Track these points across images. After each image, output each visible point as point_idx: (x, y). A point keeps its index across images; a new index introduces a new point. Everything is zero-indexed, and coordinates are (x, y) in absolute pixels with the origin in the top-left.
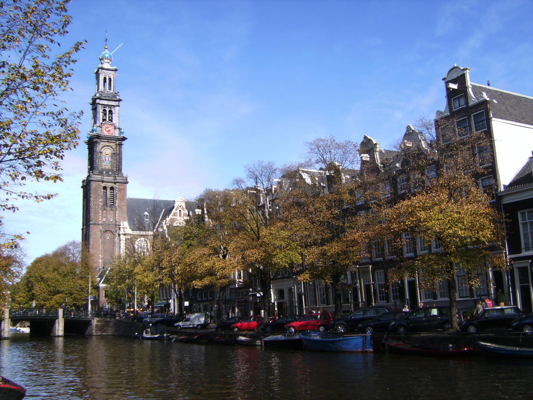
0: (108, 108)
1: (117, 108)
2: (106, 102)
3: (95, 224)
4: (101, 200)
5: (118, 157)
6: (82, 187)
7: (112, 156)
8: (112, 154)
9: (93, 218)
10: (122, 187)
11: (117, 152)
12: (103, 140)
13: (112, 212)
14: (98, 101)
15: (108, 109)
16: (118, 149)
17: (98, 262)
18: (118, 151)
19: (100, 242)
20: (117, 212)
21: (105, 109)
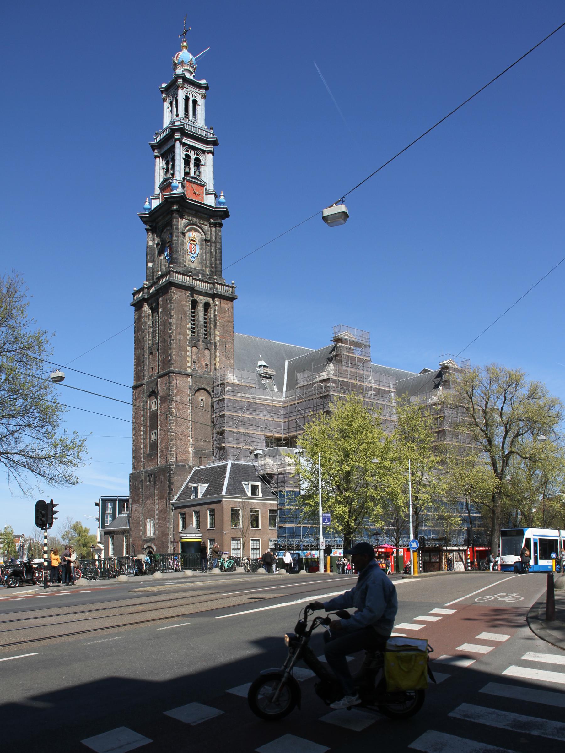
0: (193, 152)
1: (210, 155)
3: (180, 373)
4: (189, 326)
5: (213, 248)
7: (201, 245)
8: (202, 241)
9: (175, 361)
10: (226, 305)
11: (211, 237)
12: (187, 210)
13: (207, 352)
14: (177, 136)
15: (193, 156)
16: (213, 233)
17: (187, 452)
18: (214, 238)
19: (189, 411)
20: (218, 354)
21: (189, 153)
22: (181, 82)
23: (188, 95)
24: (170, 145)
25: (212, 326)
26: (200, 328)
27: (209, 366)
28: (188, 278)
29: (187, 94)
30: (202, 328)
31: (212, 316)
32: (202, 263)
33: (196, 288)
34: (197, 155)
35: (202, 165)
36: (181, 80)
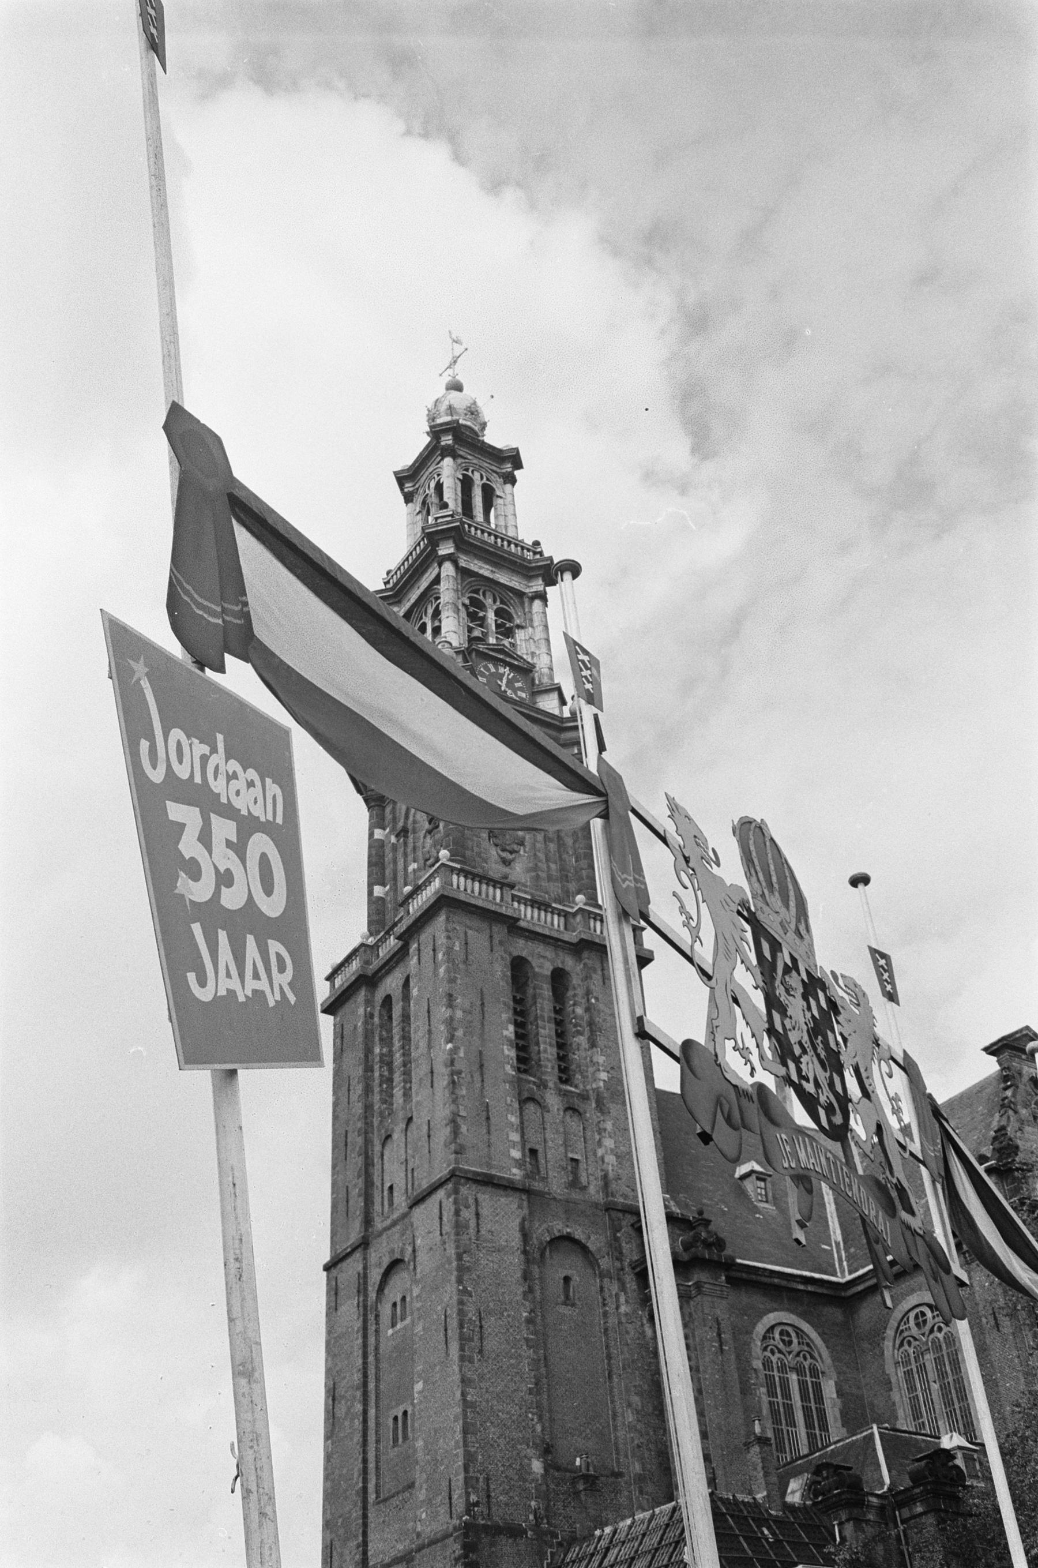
1: (537, 604)
2: (485, 570)
4: (510, 1031)
22: (450, 442)
23: (470, 474)
24: (424, 583)
25: (582, 1040)
26: (545, 1043)
27: (582, 1166)
28: (498, 891)
29: (467, 470)
30: (551, 1045)
31: (579, 1011)
32: (535, 868)
33: (522, 924)
34: (502, 602)
35: (519, 627)
36: (450, 437)
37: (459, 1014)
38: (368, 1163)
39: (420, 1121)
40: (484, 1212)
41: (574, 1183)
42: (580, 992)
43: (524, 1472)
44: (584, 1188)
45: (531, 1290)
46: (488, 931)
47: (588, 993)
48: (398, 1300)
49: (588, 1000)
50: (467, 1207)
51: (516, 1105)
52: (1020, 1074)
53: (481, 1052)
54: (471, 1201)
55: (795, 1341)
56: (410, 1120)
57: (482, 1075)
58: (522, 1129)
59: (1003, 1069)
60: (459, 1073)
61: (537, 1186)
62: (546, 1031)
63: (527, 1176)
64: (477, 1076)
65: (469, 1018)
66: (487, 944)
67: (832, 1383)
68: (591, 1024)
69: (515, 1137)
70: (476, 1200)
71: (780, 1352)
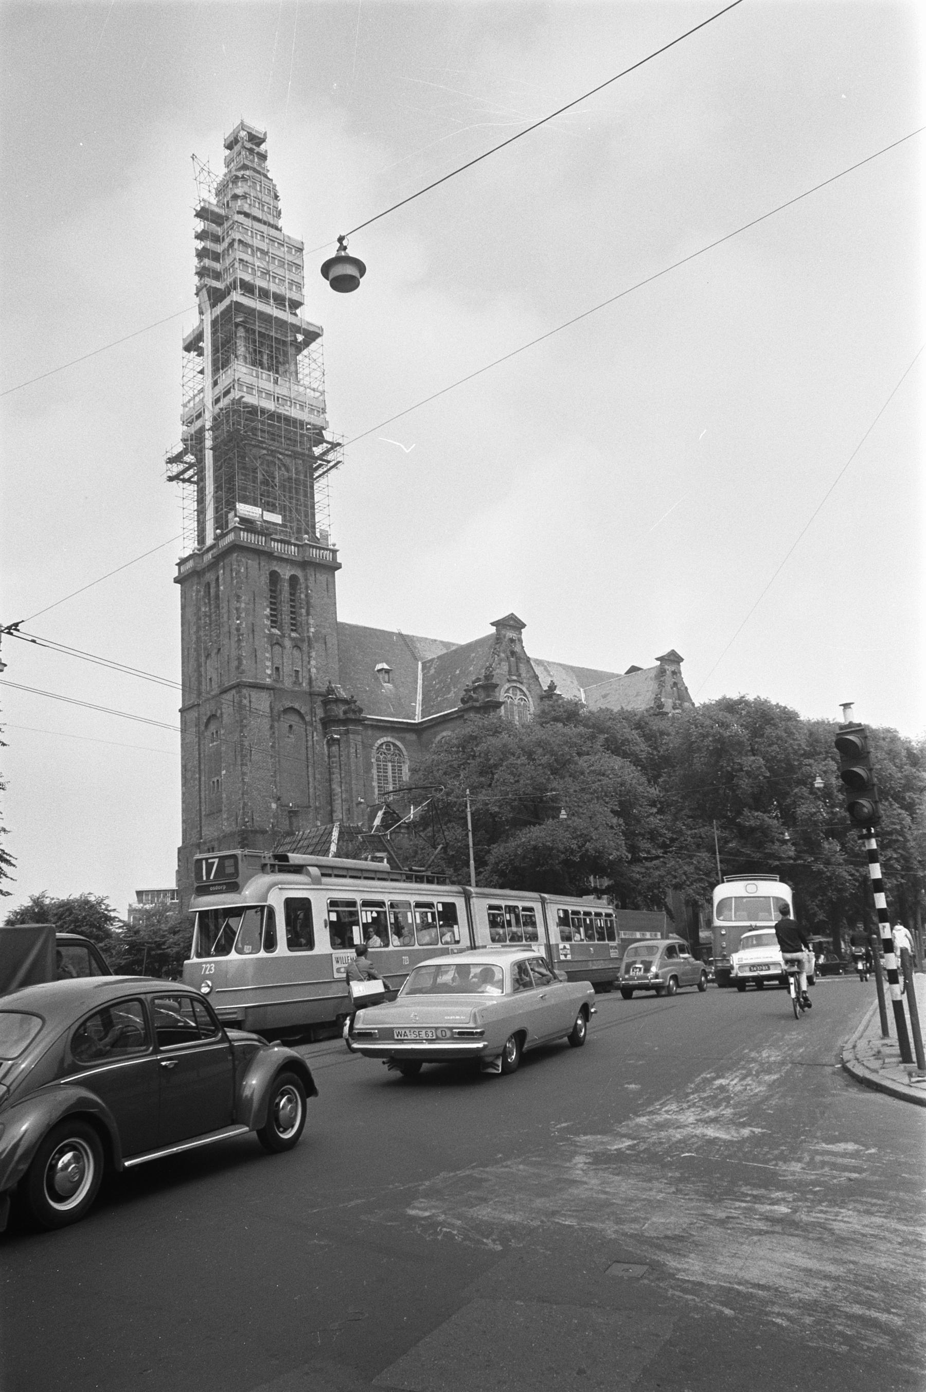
6: (177, 581)
25: (303, 611)
27: (300, 673)
31: (303, 596)
33: (276, 554)
37: (243, 605)
38: (199, 666)
39: (225, 652)
40: (253, 700)
41: (296, 683)
42: (303, 586)
43: (268, 808)
44: (300, 684)
45: (274, 733)
46: (258, 561)
47: (307, 588)
48: (215, 731)
49: (307, 591)
50: (245, 698)
51: (269, 648)
52: (505, 637)
53: (253, 624)
54: (247, 695)
55: (392, 749)
56: (219, 649)
57: (253, 634)
58: (272, 660)
59: (497, 635)
60: (243, 634)
61: (278, 686)
62: (286, 608)
63: (276, 681)
64: (251, 636)
65: (248, 606)
66: (257, 566)
67: (407, 766)
68: (308, 603)
69: (268, 664)
70: (250, 695)
71: (385, 753)
